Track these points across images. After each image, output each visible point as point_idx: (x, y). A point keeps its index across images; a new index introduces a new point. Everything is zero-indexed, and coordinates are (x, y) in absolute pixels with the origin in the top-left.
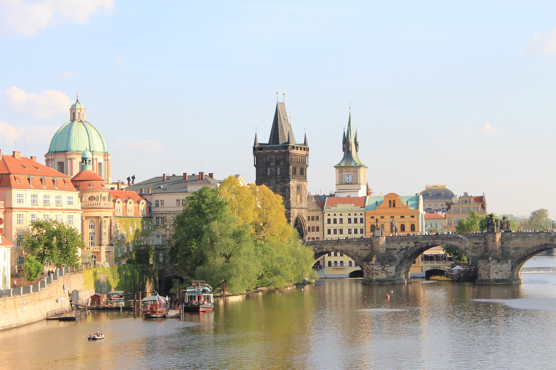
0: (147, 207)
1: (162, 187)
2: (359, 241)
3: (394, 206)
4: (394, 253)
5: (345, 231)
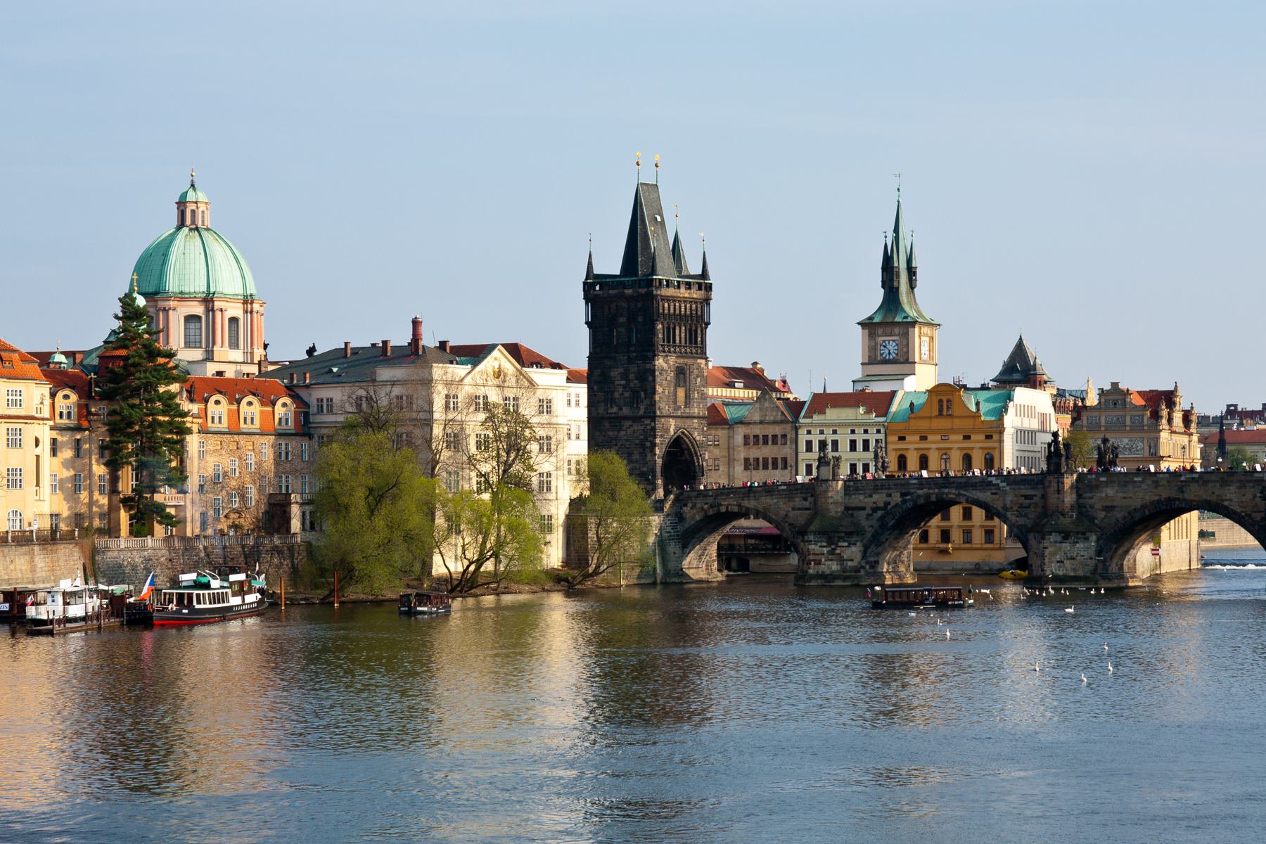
1: (335, 370)
2: (790, 490)
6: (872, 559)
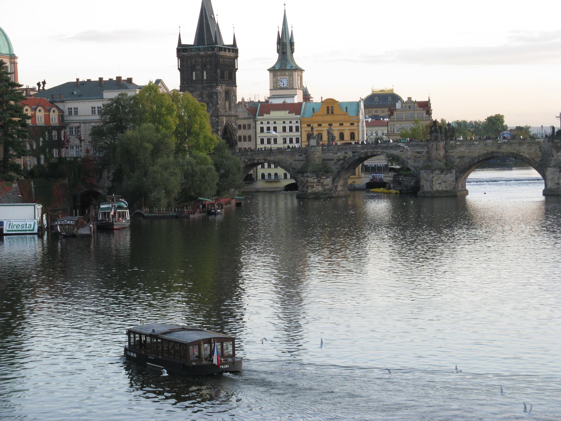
0: (59, 115)
1: (75, 93)
3: (332, 113)
4: (331, 164)
5: (280, 141)
6: (335, 184)
